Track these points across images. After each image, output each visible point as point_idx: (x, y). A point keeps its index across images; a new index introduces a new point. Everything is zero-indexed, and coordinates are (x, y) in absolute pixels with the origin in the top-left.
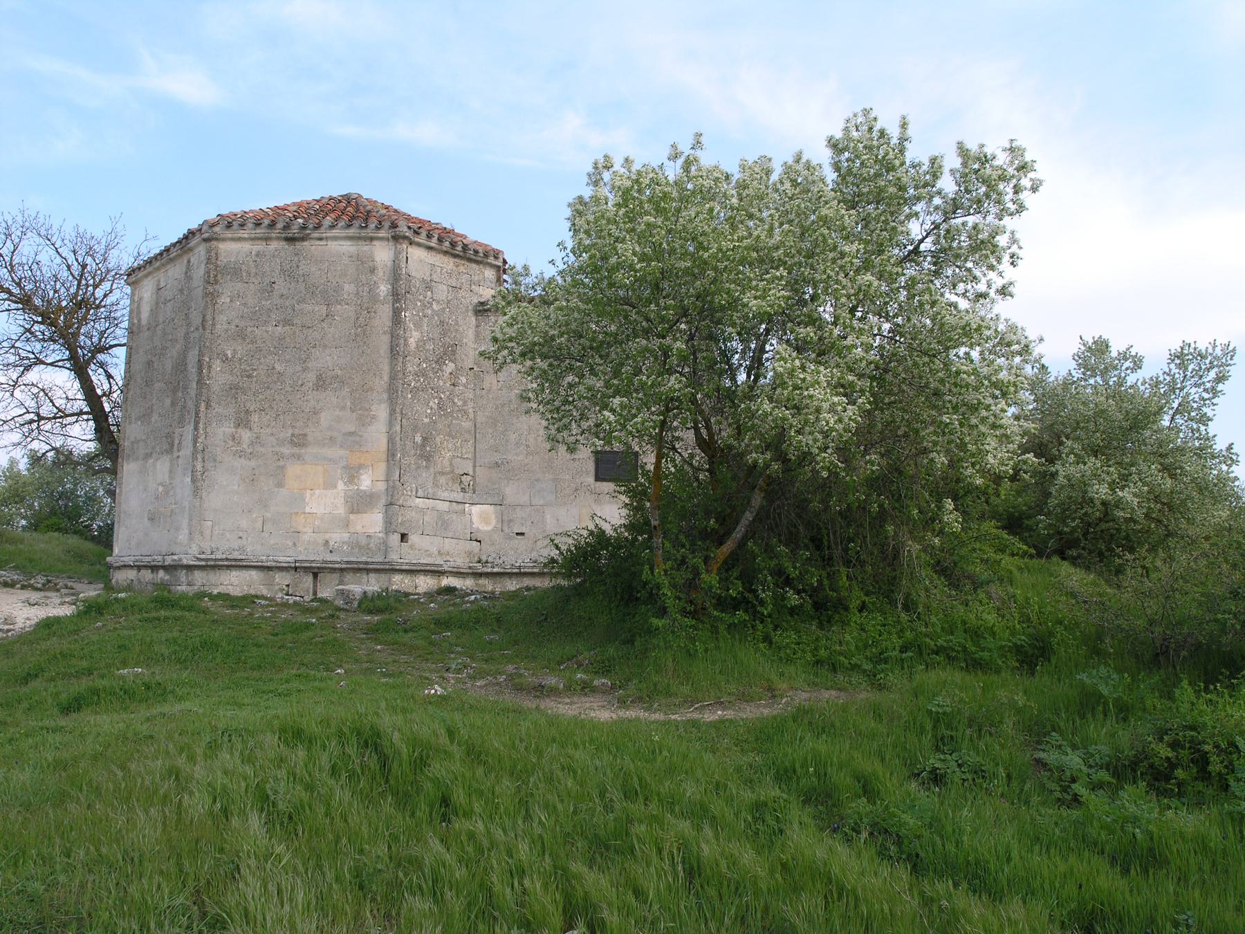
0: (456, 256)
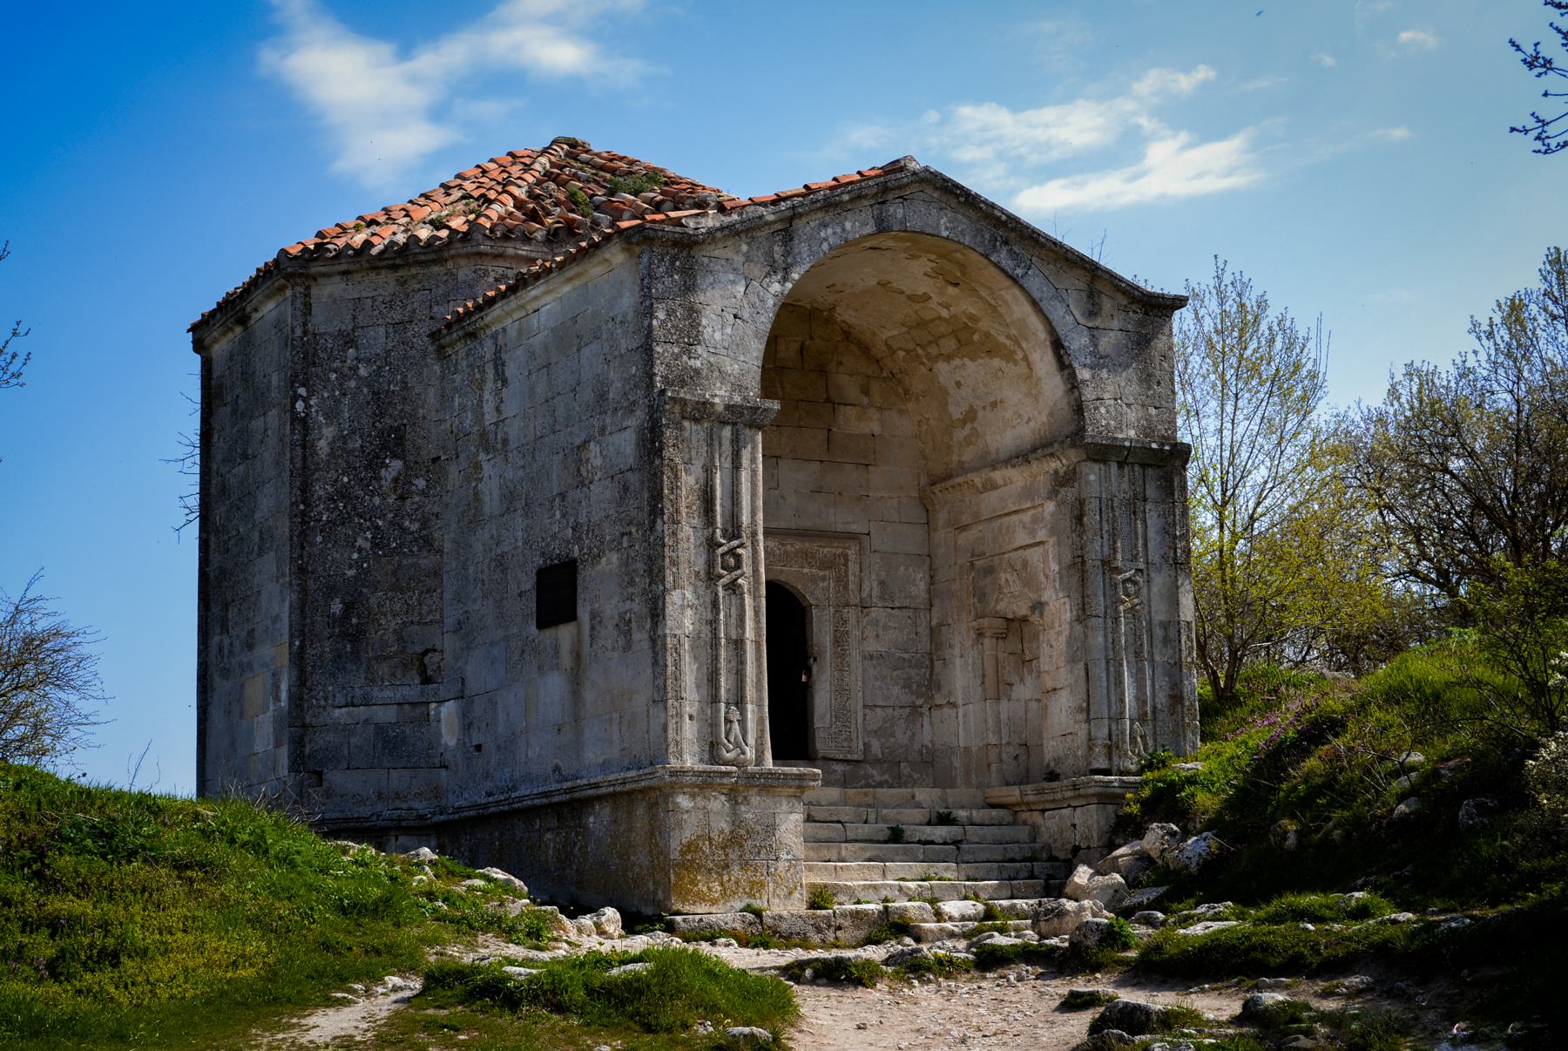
0: (395, 268)
